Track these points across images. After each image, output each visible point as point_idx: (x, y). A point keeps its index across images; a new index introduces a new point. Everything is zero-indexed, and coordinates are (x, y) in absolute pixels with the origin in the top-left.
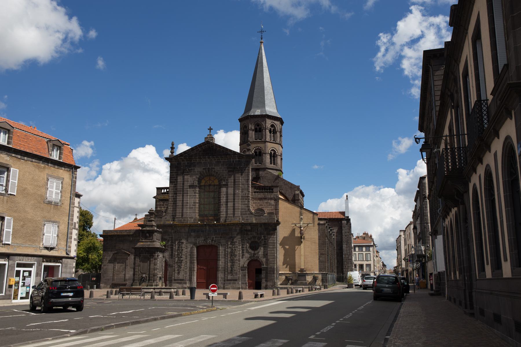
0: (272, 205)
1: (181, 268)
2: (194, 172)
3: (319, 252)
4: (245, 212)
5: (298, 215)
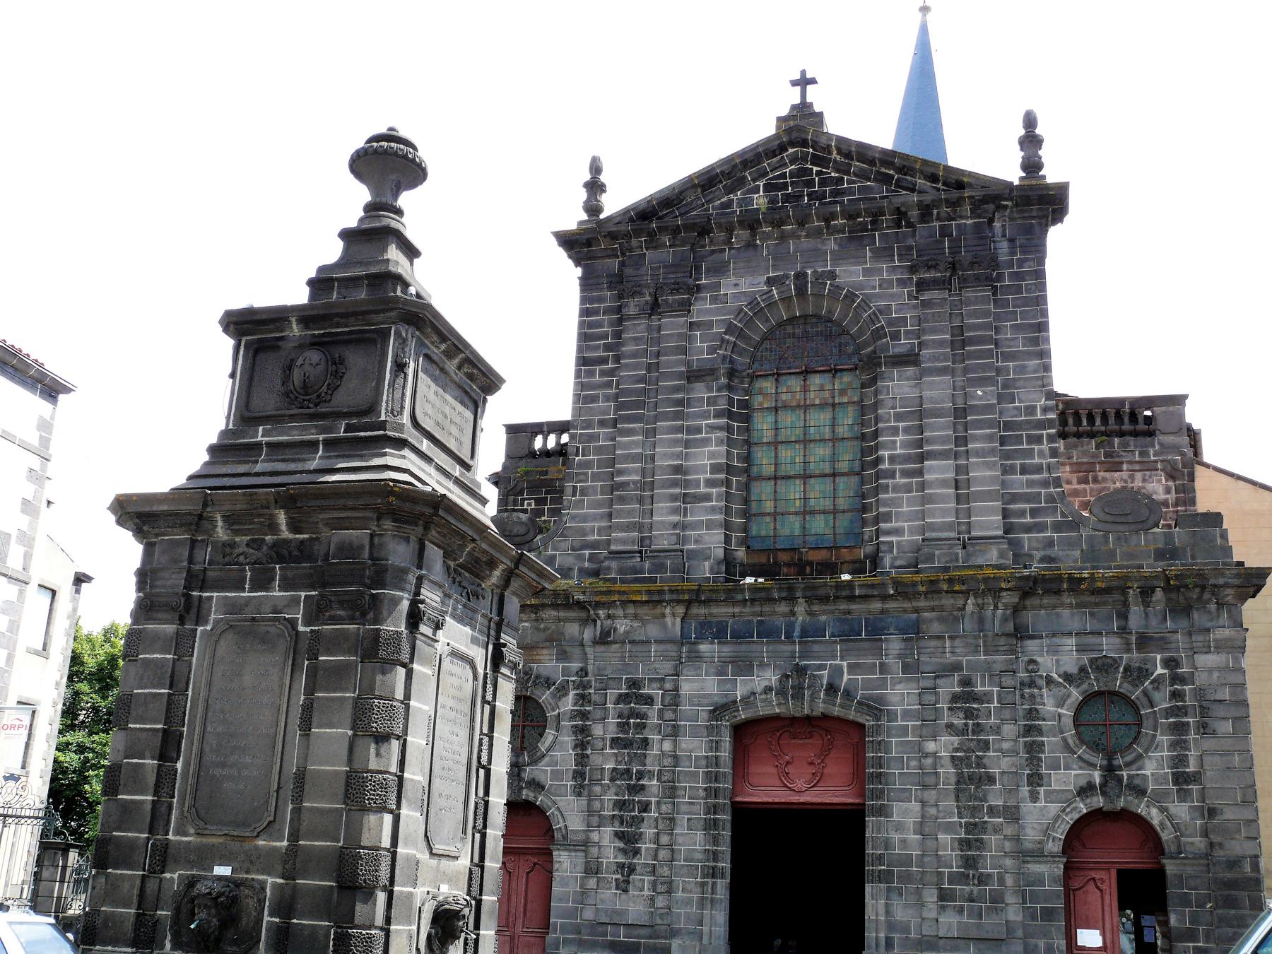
1: (636, 852)
2: (715, 299)
4: (1034, 513)
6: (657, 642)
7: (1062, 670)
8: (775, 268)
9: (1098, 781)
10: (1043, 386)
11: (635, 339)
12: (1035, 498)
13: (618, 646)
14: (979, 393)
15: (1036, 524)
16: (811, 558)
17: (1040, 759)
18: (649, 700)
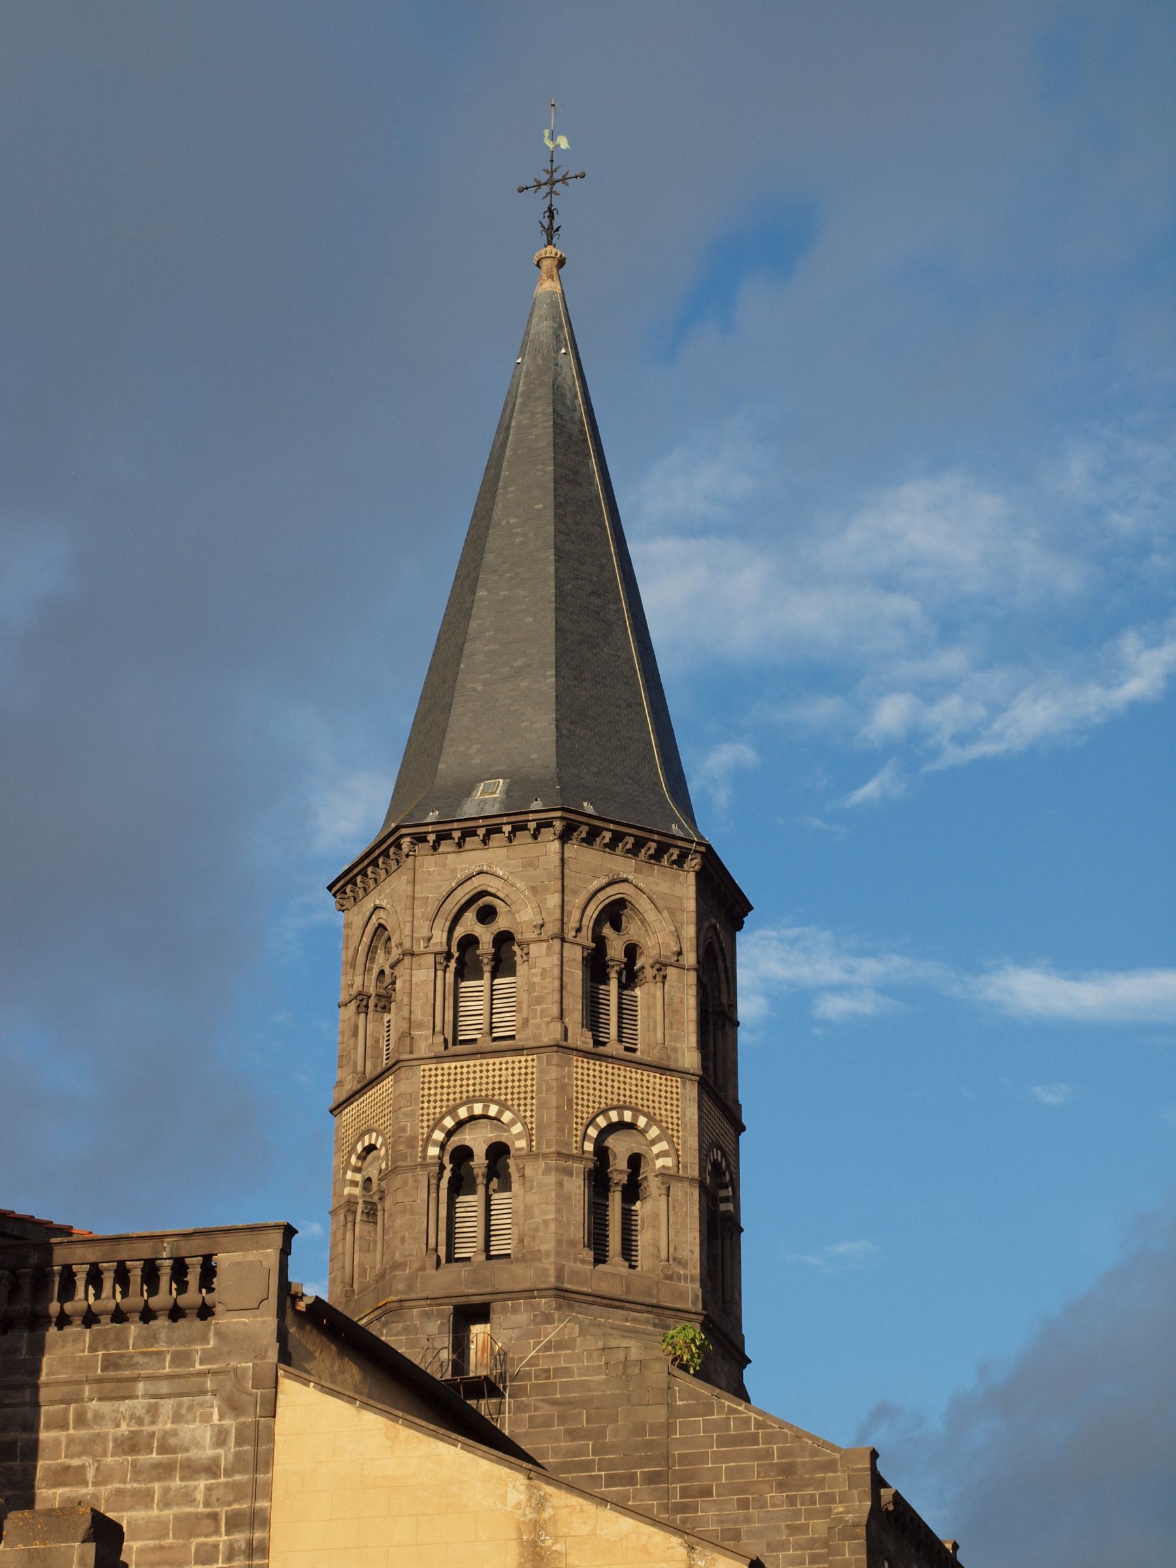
0: (192, 1470)
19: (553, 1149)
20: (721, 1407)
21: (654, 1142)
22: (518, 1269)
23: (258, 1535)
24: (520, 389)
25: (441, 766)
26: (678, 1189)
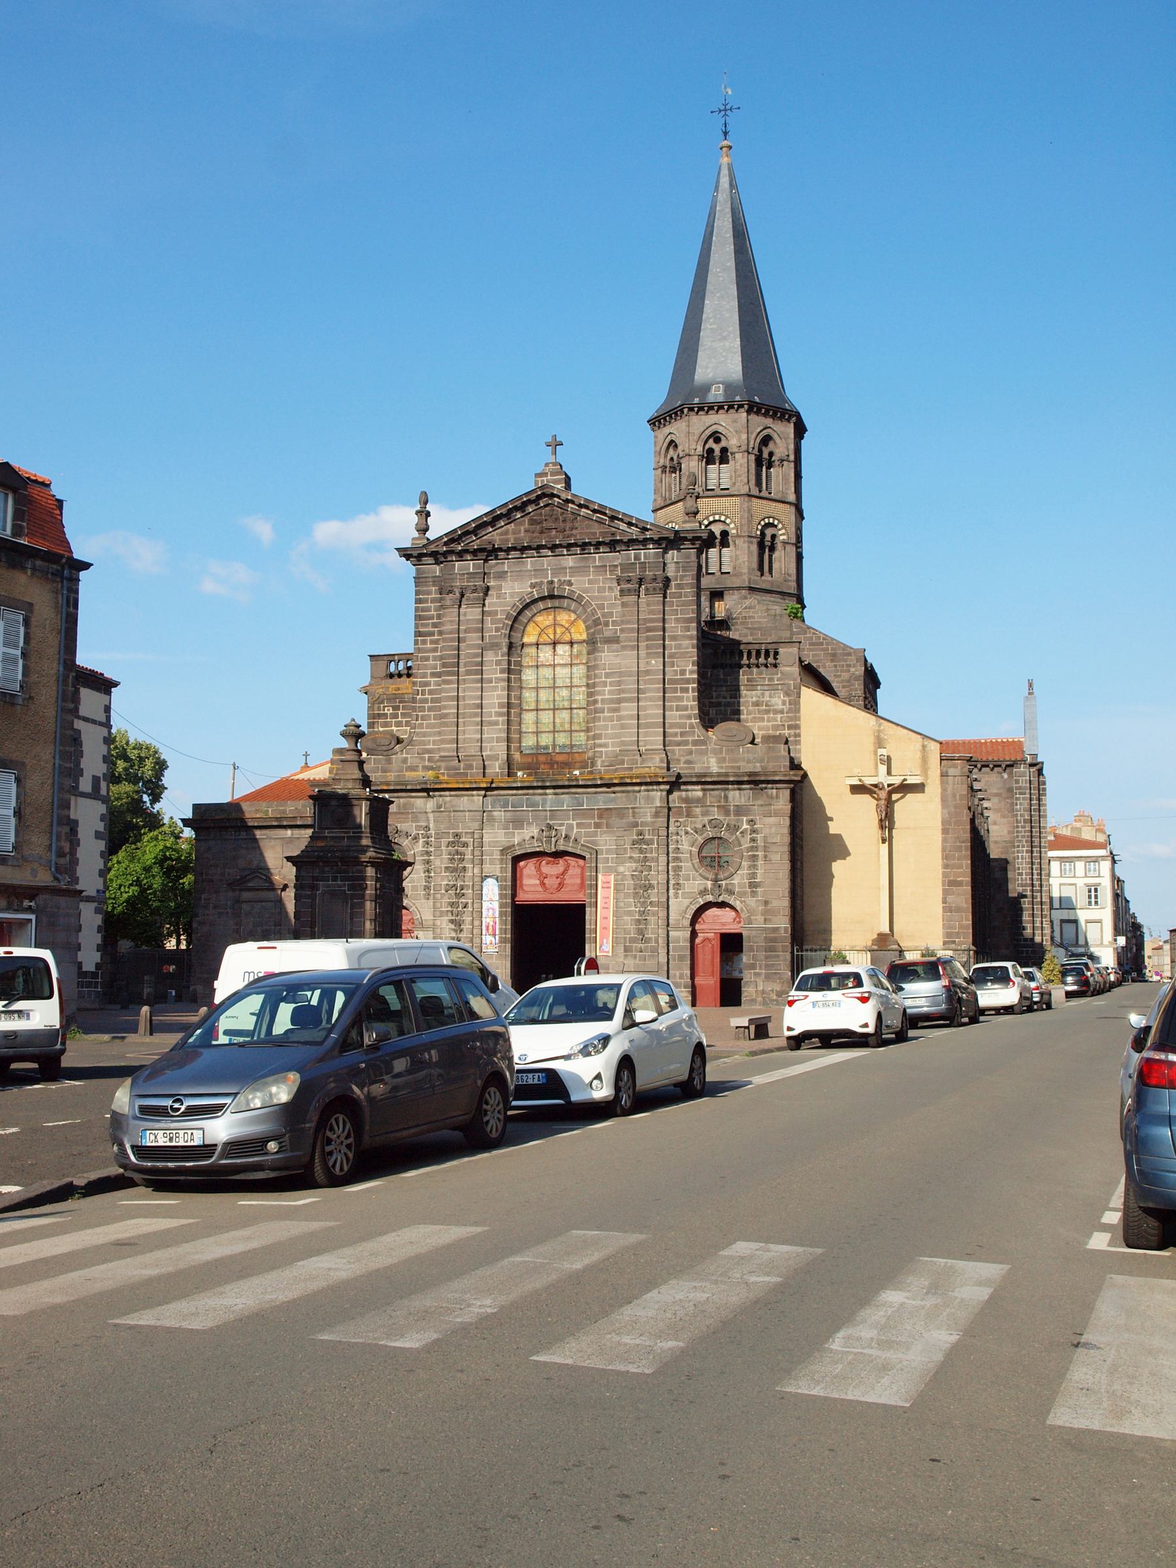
0: (776, 712)
3: (945, 875)
4: (682, 734)
5: (870, 741)
6: (469, 811)
7: (693, 826)
8: (536, 578)
9: (709, 887)
10: (691, 657)
11: (451, 621)
12: (683, 726)
13: (447, 813)
14: (653, 662)
15: (683, 741)
16: (557, 759)
17: (679, 875)
18: (465, 845)
19: (746, 534)
20: (810, 632)
21: (780, 530)
22: (735, 579)
23: (797, 731)
24: (718, 208)
25: (696, 377)
26: (788, 547)
